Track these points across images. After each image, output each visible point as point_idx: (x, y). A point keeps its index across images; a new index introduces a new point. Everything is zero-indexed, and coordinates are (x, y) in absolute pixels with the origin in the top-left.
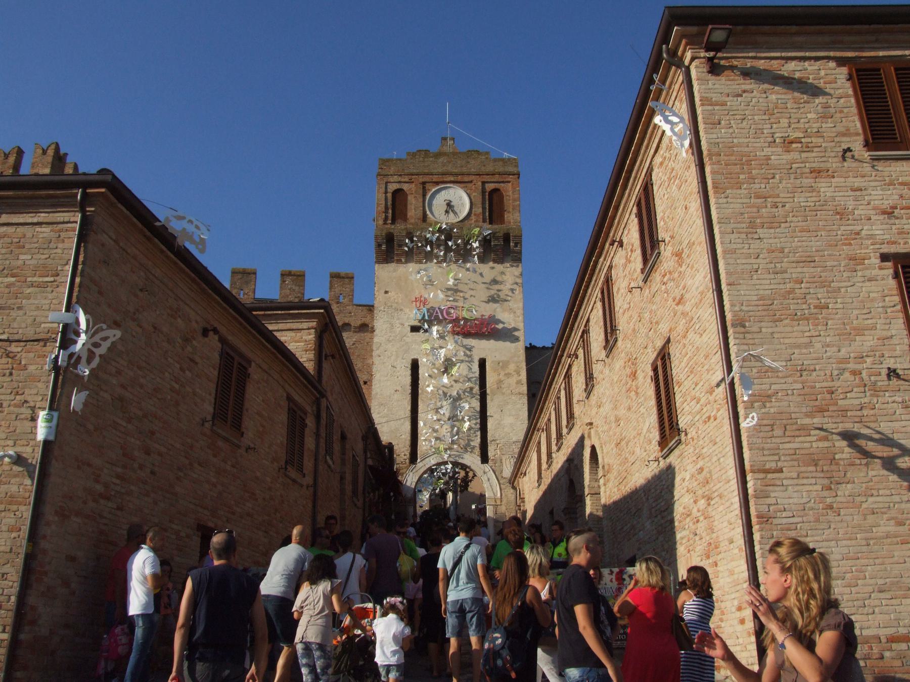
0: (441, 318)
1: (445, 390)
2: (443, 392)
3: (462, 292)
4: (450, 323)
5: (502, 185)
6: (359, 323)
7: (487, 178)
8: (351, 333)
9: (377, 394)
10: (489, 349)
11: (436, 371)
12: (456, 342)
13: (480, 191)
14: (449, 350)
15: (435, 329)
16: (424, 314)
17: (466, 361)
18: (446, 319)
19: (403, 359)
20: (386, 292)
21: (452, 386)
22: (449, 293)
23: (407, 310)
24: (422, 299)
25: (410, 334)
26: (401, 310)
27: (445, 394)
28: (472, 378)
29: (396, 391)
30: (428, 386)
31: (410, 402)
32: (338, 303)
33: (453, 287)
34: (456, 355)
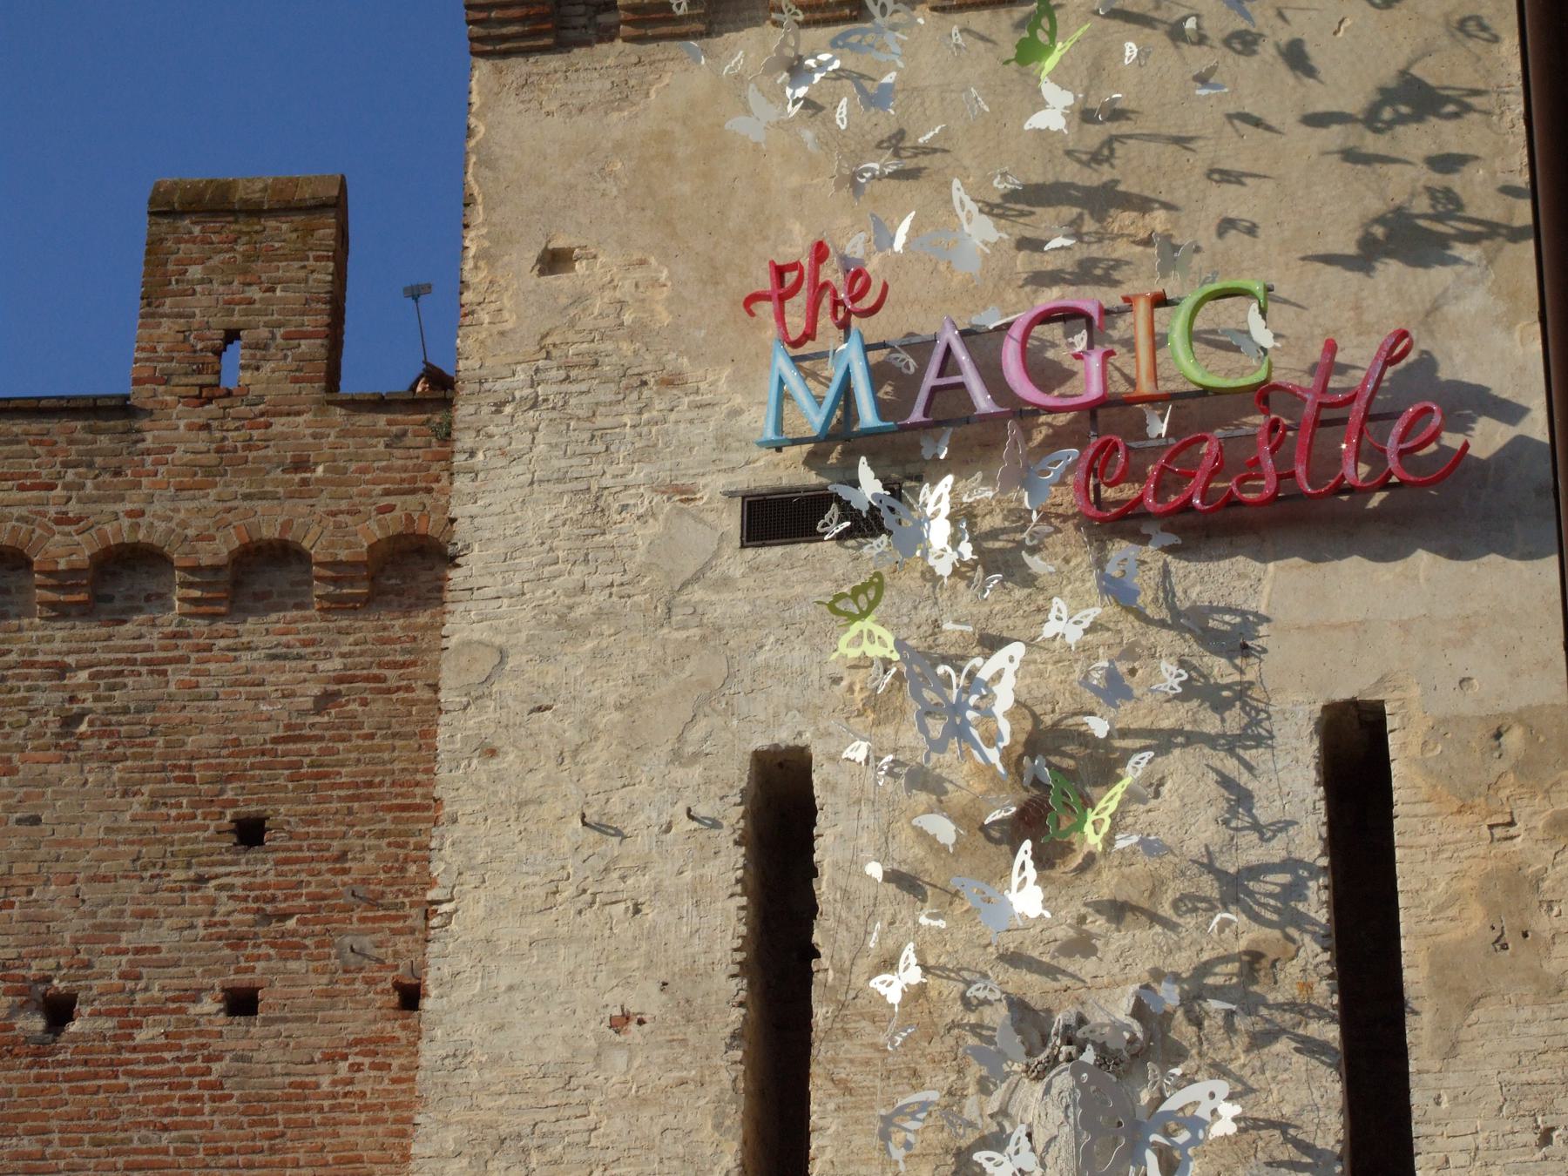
0: (983, 402)
1: (1033, 987)
2: (1019, 1008)
3: (1143, 205)
4: (1057, 440)
6: (370, 532)
8: (310, 622)
9: (459, 1057)
10: (1405, 627)
11: (944, 830)
12: (1119, 592)
14: (1066, 657)
15: (937, 497)
16: (846, 392)
17: (1211, 741)
18: (1025, 414)
19: (677, 757)
20: (554, 261)
21: (1082, 945)
22: (1046, 218)
23: (717, 381)
24: (831, 273)
25: (738, 561)
26: (671, 381)
27: (1026, 1016)
28: (1256, 871)
29: (621, 1022)
30: (889, 964)
31: (735, 1114)
32: (204, 396)
33: (1071, 173)
34: (1115, 689)
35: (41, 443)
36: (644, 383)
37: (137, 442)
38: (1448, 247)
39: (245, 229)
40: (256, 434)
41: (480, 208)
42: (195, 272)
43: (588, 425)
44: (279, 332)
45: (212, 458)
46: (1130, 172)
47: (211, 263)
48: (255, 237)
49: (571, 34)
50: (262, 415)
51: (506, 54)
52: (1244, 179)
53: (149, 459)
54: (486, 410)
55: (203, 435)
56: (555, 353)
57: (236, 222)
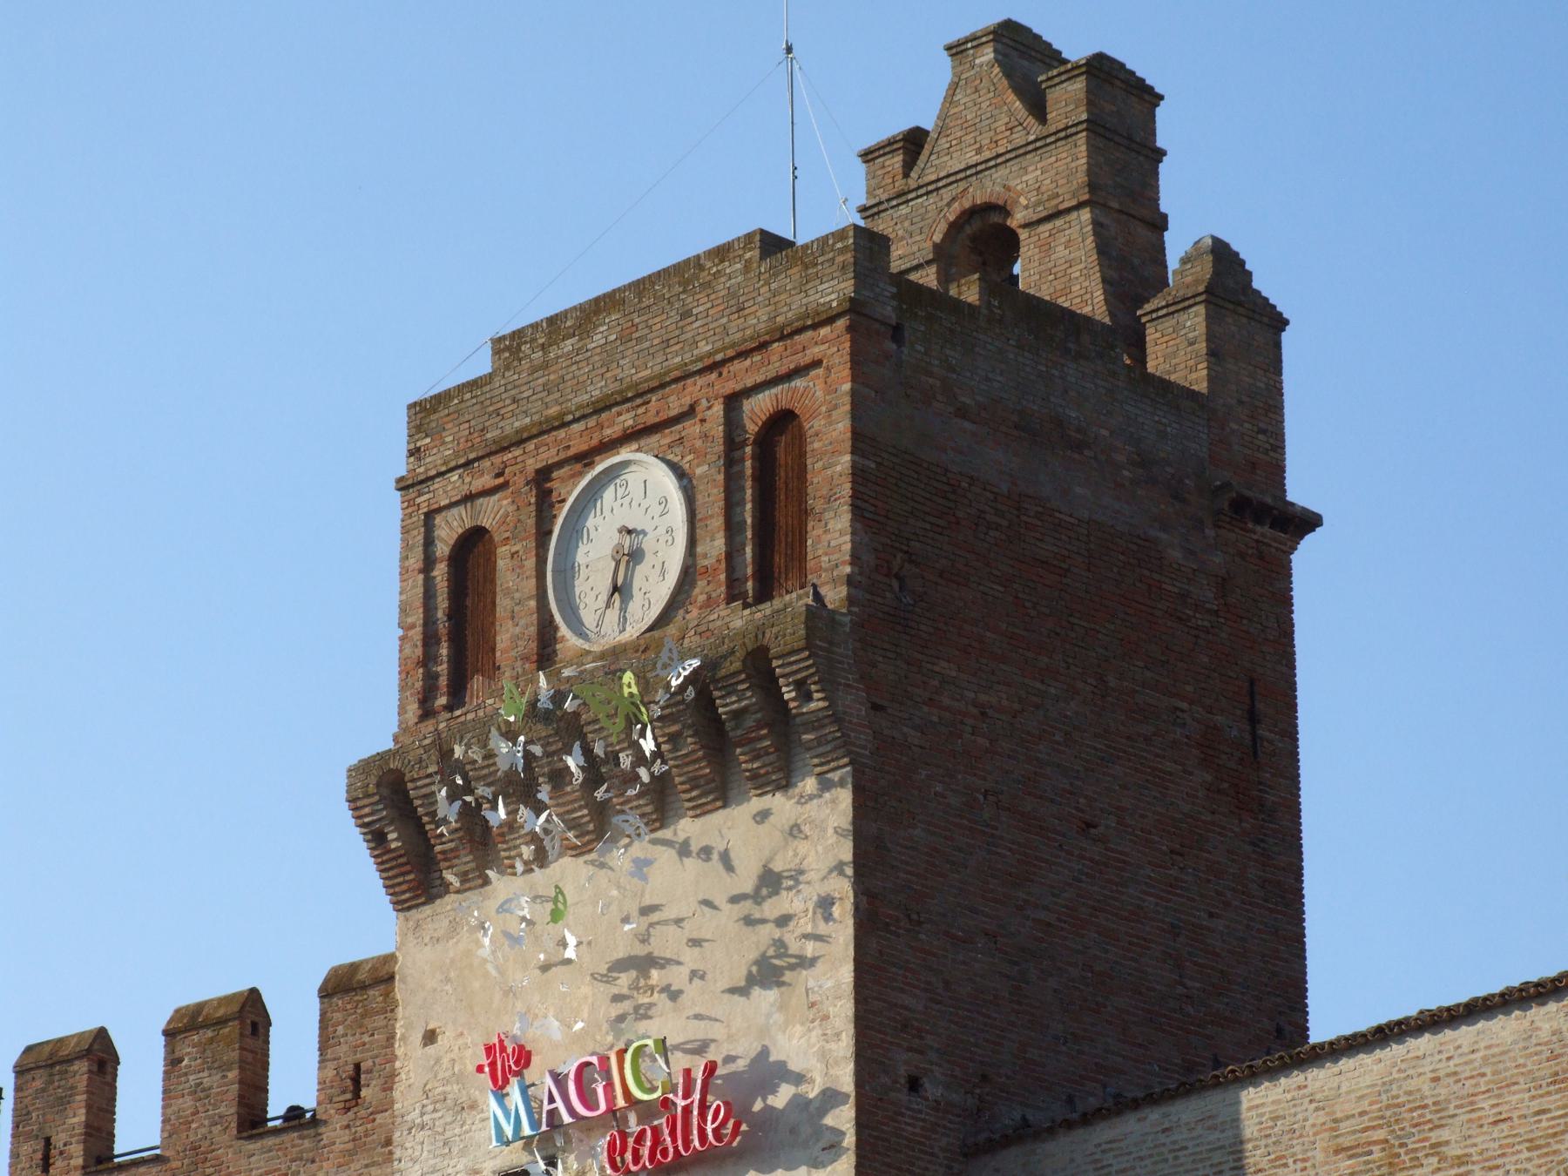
0: (567, 1119)
5: (799, 383)
7: (743, 374)
13: (719, 447)
20: (430, 1037)
35: (279, 1149)
36: (463, 1108)
37: (319, 1141)
38: (783, 975)
39: (360, 998)
40: (369, 1126)
41: (400, 1008)
42: (340, 1030)
43: (442, 1137)
44: (377, 1061)
45: (350, 1146)
46: (657, 947)
47: (346, 1023)
48: (365, 1002)
49: (435, 891)
50: (372, 1114)
51: (409, 909)
52: (704, 944)
53: (325, 1150)
54: (405, 1133)
55: (347, 1131)
56: (430, 1094)
57: (356, 995)
